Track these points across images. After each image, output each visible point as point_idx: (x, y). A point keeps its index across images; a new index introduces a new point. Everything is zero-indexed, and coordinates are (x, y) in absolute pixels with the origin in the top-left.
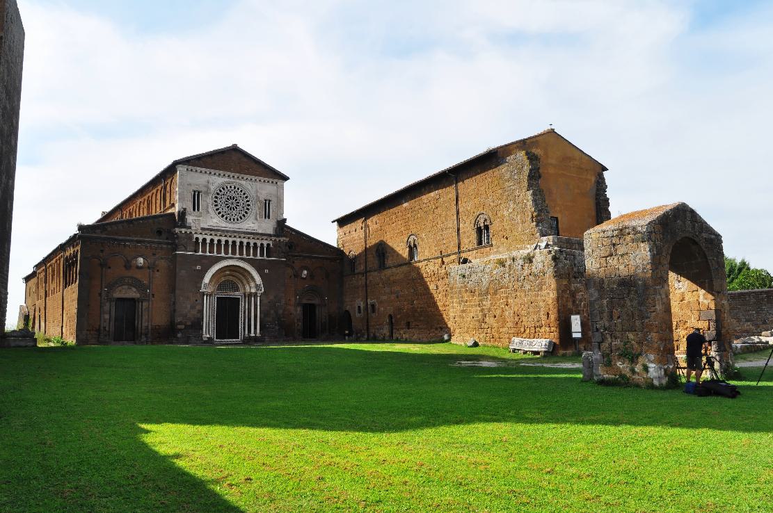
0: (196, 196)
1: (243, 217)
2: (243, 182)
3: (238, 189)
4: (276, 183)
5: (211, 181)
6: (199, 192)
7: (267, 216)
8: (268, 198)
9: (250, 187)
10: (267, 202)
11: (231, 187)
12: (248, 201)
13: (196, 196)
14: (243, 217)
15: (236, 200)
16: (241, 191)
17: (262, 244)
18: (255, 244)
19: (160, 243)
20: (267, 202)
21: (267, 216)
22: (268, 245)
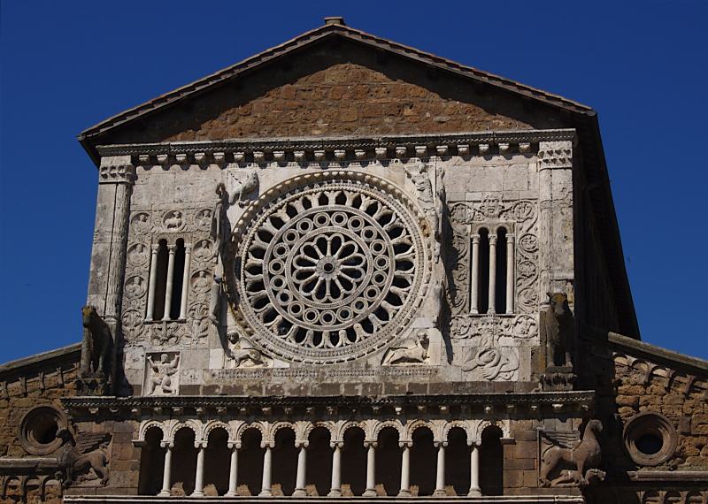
0: (171, 257)
1: (376, 322)
2: (375, 170)
3: (357, 203)
4: (534, 149)
5: (233, 188)
6: (180, 242)
7: (494, 300)
8: (493, 224)
9: (409, 190)
10: (493, 237)
11: (323, 200)
12: (402, 248)
13: (171, 257)
14: (376, 322)
15: (349, 249)
16: (371, 210)
17: (457, 436)
18: (423, 436)
19: (32, 471)
20: (493, 237)
21: (494, 300)
22: (492, 435)
